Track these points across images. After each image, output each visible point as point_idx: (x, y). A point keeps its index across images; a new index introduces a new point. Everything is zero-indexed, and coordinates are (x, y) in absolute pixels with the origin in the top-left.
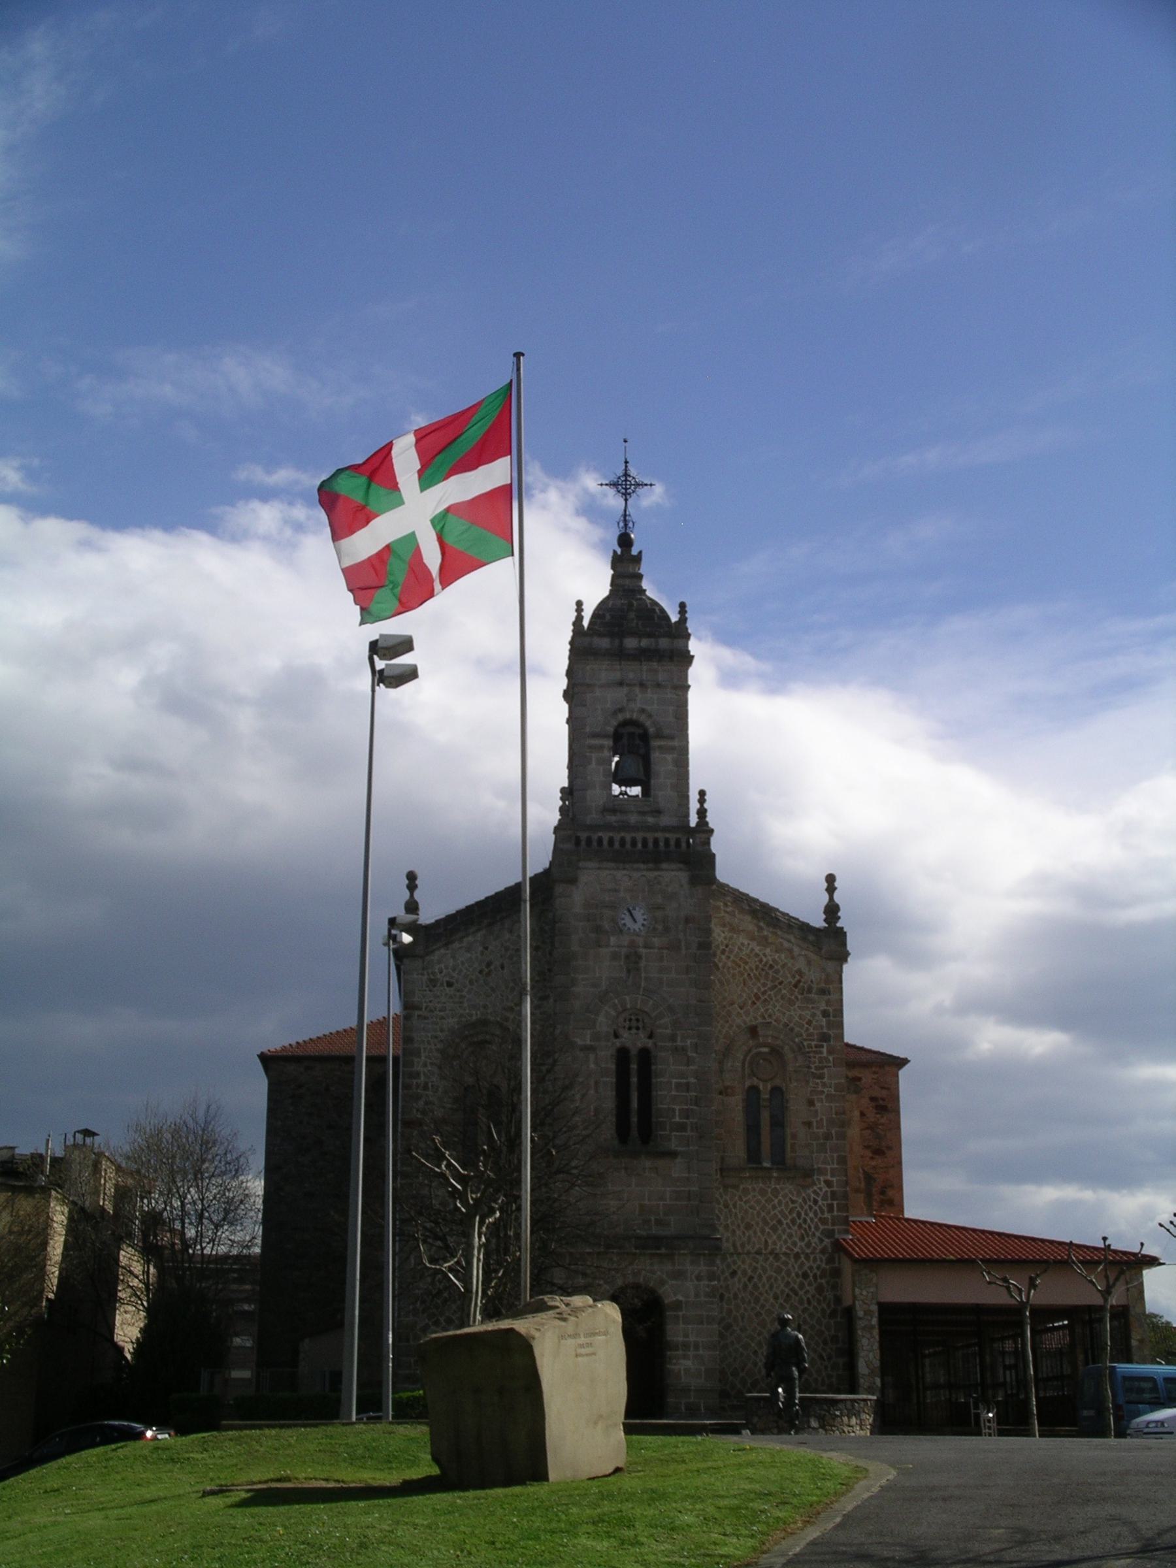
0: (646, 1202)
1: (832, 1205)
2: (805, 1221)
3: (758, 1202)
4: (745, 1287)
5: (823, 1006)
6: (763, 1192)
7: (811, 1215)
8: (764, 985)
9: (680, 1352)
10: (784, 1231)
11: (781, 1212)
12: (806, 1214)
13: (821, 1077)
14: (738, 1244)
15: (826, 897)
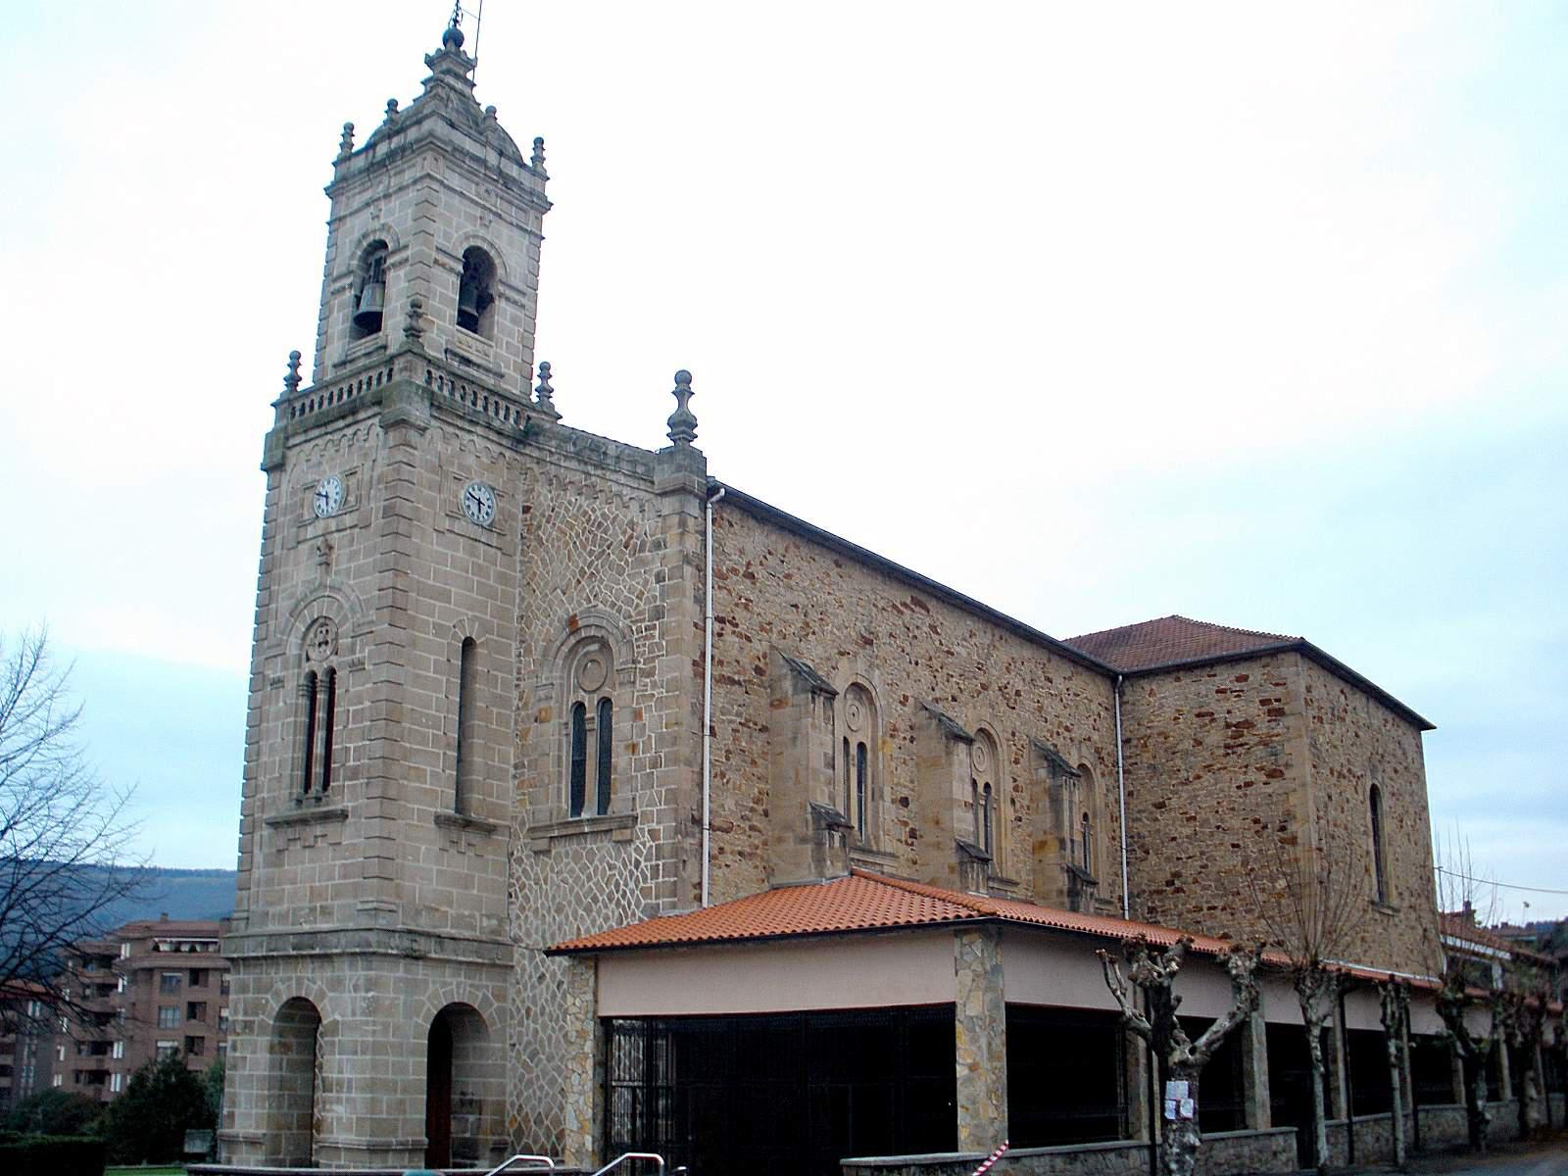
0: (317, 884)
1: (658, 865)
2: (624, 895)
3: (572, 871)
4: (554, 996)
5: (656, 567)
6: (577, 858)
7: (632, 885)
8: (591, 553)
9: (334, 1094)
10: (599, 912)
11: (597, 884)
12: (626, 885)
13: (650, 674)
14: (547, 936)
15: (673, 404)
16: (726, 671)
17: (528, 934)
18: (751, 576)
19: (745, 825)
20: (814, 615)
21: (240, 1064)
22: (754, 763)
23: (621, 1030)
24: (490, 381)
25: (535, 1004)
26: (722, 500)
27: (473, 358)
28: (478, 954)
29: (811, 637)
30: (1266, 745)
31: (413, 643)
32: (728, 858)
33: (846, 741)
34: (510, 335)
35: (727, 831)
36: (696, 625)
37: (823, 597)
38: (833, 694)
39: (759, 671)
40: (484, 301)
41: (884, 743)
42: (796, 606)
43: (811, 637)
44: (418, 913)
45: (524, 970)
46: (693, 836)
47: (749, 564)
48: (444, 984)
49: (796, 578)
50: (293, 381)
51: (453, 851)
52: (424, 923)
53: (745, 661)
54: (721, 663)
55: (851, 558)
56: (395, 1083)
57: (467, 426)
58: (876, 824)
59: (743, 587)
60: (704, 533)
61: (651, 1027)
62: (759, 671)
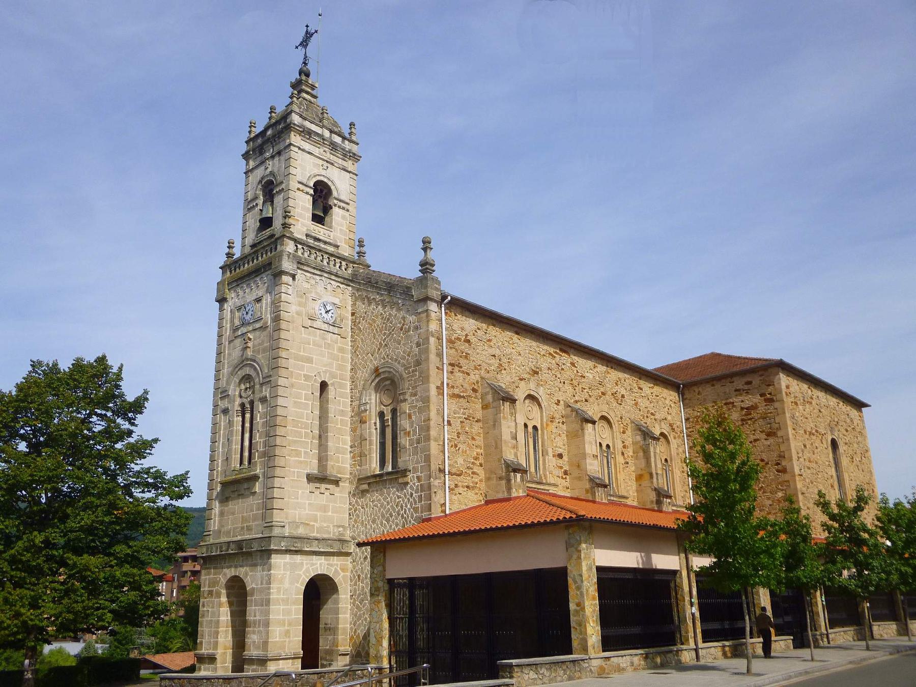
3: (380, 500)
15: (421, 255)
16: (456, 391)
17: (359, 536)
18: (468, 341)
19: (470, 472)
20: (504, 360)
21: (206, 614)
22: (473, 439)
23: (400, 586)
24: (331, 249)
25: (362, 573)
26: (450, 302)
27: (321, 238)
28: (331, 546)
29: (503, 372)
30: (764, 418)
31: (292, 386)
32: (460, 490)
33: (526, 426)
34: (342, 226)
35: (459, 475)
36: (438, 368)
37: (508, 351)
38: (513, 401)
39: (474, 390)
40: (327, 209)
41: (547, 425)
42: (494, 356)
43: (503, 372)
44: (298, 527)
45: (357, 554)
46: (440, 478)
47: (467, 335)
48: (313, 565)
49: (494, 341)
50: (229, 255)
51: (317, 492)
52: (301, 531)
53: (466, 385)
54: (453, 387)
55: (525, 330)
56: (284, 621)
57: (318, 272)
58: (544, 468)
59: (464, 347)
60: (441, 320)
61: (412, 583)
62: (474, 390)
